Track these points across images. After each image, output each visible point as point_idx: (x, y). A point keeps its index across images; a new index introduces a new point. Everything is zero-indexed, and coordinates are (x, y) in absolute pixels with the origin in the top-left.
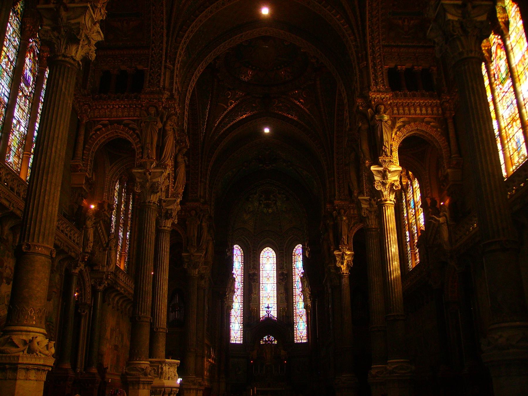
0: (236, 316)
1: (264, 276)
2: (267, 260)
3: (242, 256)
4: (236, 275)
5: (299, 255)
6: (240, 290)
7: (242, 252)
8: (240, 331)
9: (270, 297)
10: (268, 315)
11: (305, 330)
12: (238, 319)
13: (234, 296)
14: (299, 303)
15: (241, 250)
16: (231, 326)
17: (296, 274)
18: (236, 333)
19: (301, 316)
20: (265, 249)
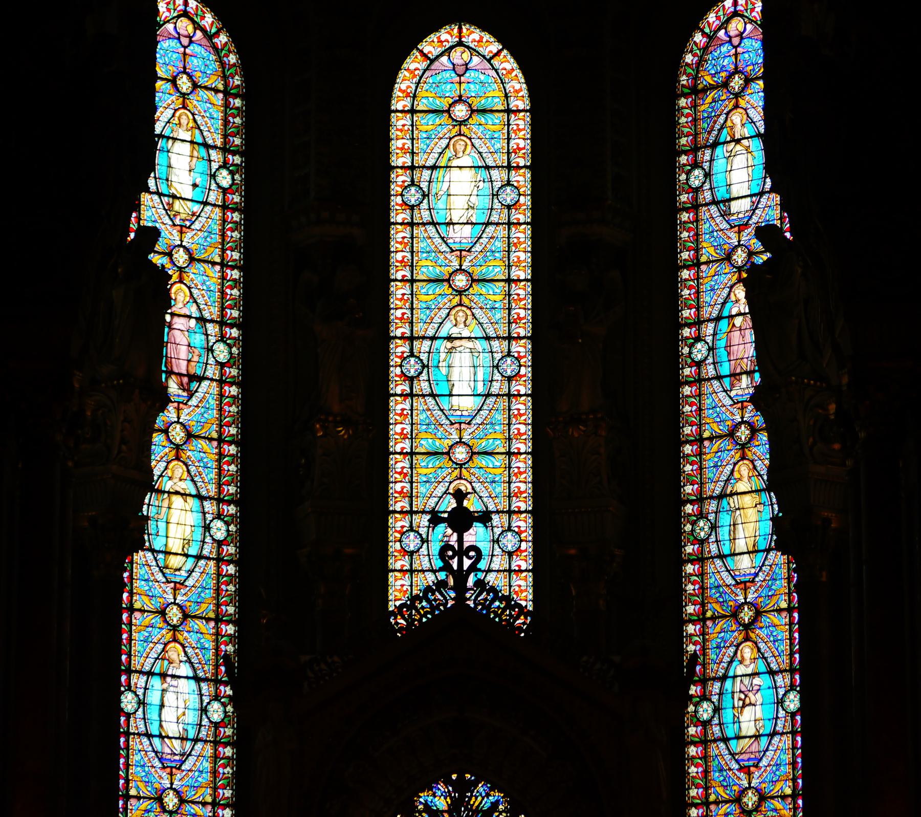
0: (174, 615)
1: (426, 269)
2: (447, 129)
3: (226, 93)
4: (181, 257)
5: (737, 83)
6: (214, 388)
7: (233, 59)
8: (209, 750)
9: (473, 454)
10: (460, 587)
11: (786, 742)
12: (192, 638)
13: (158, 438)
14: (734, 501)
15: (223, 39)
16: (128, 702)
17: (708, 251)
18: (172, 766)
19: (747, 615)
20: (433, 37)
